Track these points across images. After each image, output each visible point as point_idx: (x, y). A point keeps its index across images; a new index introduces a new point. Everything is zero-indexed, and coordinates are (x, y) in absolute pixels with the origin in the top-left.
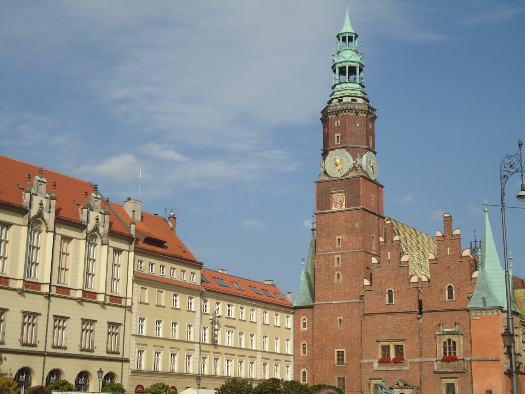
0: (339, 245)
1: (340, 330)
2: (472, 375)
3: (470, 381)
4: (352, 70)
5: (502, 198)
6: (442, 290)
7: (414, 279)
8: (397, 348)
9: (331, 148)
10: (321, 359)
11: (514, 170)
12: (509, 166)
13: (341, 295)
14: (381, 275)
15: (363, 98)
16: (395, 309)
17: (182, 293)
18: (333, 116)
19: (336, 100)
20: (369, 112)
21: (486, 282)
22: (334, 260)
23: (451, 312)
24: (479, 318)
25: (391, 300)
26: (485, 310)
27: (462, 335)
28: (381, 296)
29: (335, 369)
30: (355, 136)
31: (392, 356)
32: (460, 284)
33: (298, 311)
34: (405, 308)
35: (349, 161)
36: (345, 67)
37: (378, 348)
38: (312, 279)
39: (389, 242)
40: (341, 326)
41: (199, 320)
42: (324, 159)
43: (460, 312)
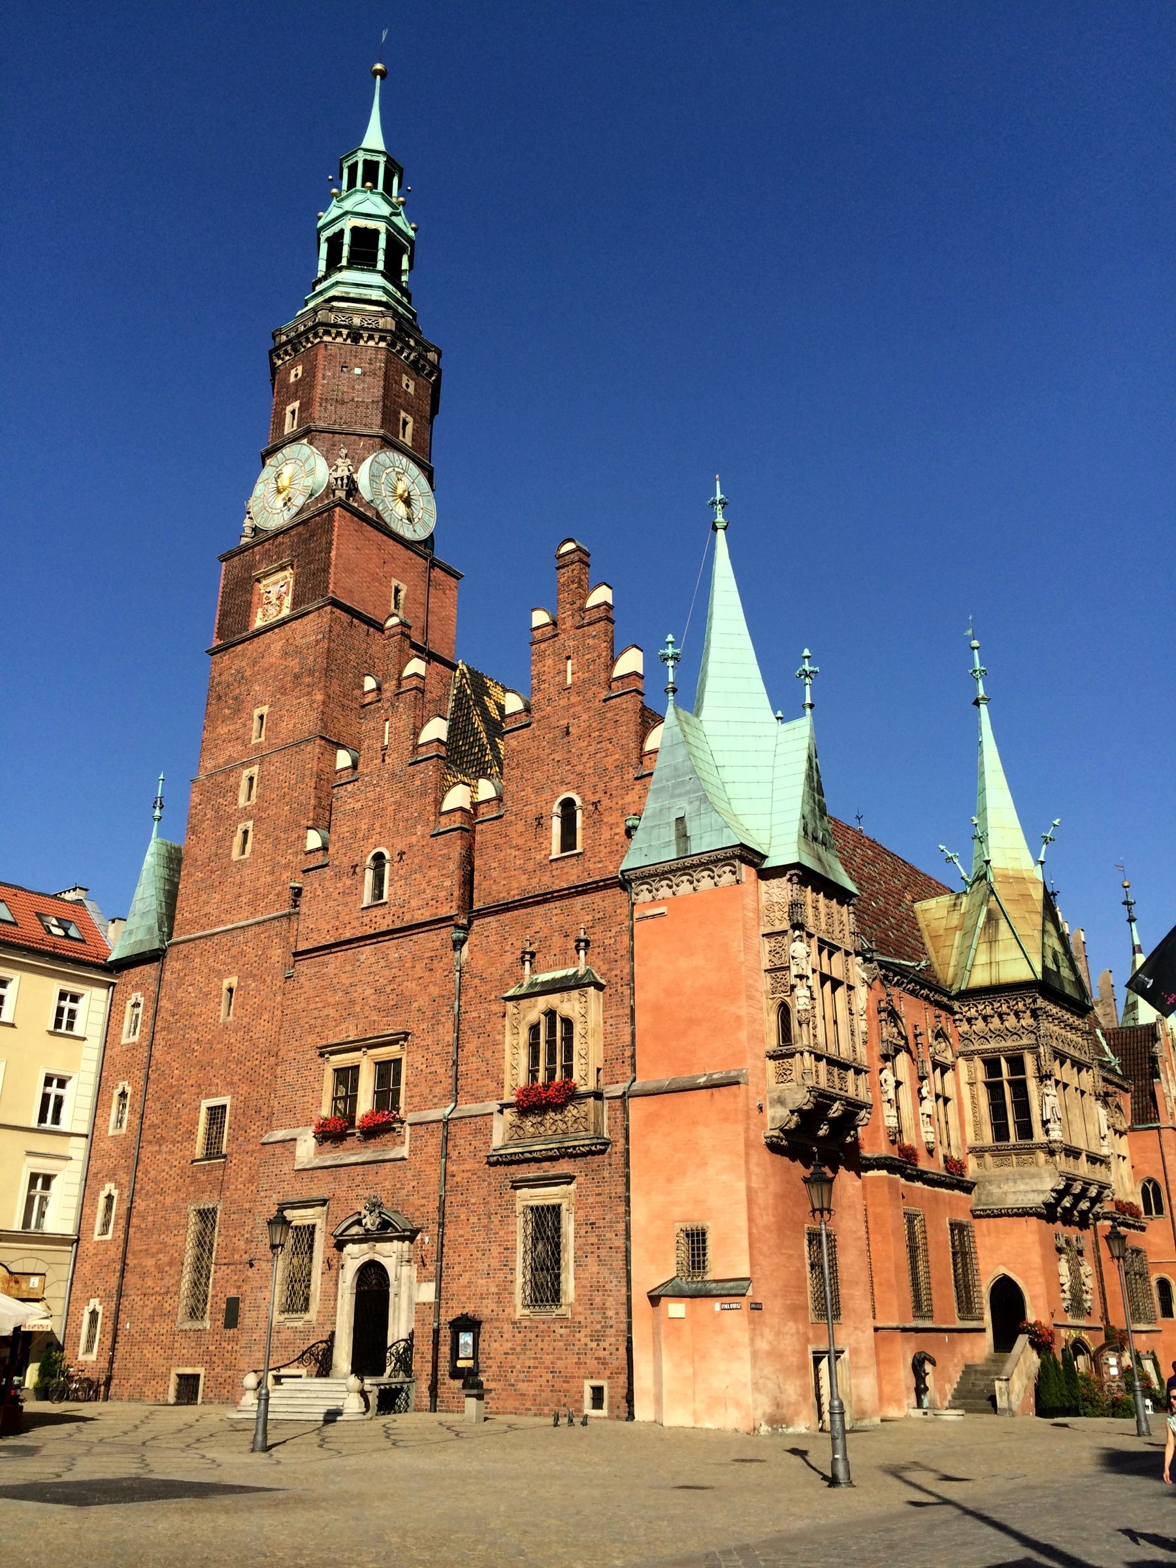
2: (627, 1165)
3: (621, 1189)
6: (539, 820)
10: (160, 1141)
16: (388, 920)
21: (690, 754)
23: (566, 902)
26: (685, 870)
27: (600, 987)
28: (349, 882)
29: (194, 1178)
30: (343, 403)
32: (601, 786)
35: (312, 472)
36: (342, 231)
37: (320, 1080)
39: (390, 687)
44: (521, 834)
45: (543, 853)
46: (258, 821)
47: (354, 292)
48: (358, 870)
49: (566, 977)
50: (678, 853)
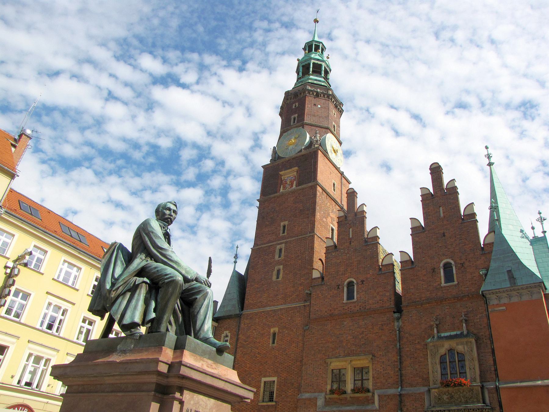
0: (284, 232)
6: (434, 270)
14: (339, 261)
22: (275, 251)
24: (504, 308)
25: (350, 296)
30: (314, 116)
36: (309, 64)
40: (273, 343)
44: (425, 275)
45: (437, 283)
47: (315, 82)
48: (340, 287)
49: (457, 335)
50: (511, 284)
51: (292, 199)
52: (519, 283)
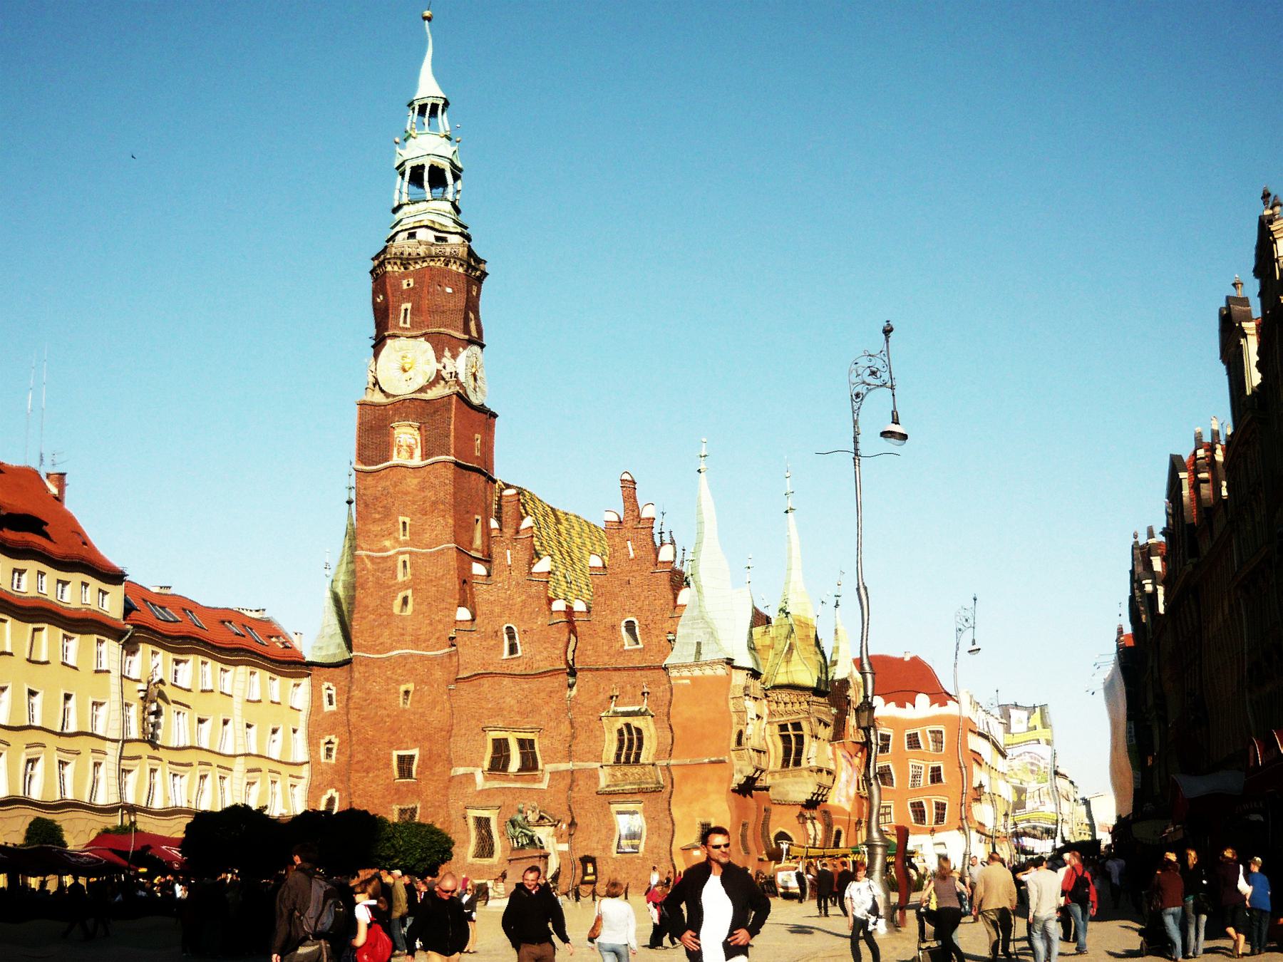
1: (405, 710)
4: (437, 178)
5: (855, 438)
6: (613, 627)
7: (559, 605)
8: (522, 743)
9: (390, 332)
11: (878, 382)
12: (868, 371)
13: (408, 638)
15: (461, 234)
17: (82, 633)
18: (396, 268)
19: (405, 234)
20: (469, 265)
22: (396, 567)
24: (688, 681)
25: (513, 649)
28: (493, 643)
31: (515, 763)
33: (316, 670)
34: (542, 664)
36: (423, 167)
38: (345, 607)
39: (509, 532)
41: (118, 689)
42: (376, 356)
43: (649, 672)
46: (415, 591)
51: (415, 481)
52: (703, 658)
